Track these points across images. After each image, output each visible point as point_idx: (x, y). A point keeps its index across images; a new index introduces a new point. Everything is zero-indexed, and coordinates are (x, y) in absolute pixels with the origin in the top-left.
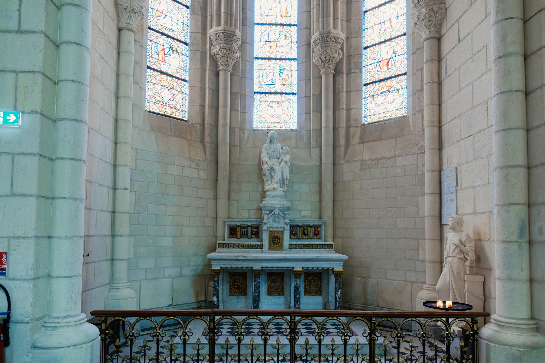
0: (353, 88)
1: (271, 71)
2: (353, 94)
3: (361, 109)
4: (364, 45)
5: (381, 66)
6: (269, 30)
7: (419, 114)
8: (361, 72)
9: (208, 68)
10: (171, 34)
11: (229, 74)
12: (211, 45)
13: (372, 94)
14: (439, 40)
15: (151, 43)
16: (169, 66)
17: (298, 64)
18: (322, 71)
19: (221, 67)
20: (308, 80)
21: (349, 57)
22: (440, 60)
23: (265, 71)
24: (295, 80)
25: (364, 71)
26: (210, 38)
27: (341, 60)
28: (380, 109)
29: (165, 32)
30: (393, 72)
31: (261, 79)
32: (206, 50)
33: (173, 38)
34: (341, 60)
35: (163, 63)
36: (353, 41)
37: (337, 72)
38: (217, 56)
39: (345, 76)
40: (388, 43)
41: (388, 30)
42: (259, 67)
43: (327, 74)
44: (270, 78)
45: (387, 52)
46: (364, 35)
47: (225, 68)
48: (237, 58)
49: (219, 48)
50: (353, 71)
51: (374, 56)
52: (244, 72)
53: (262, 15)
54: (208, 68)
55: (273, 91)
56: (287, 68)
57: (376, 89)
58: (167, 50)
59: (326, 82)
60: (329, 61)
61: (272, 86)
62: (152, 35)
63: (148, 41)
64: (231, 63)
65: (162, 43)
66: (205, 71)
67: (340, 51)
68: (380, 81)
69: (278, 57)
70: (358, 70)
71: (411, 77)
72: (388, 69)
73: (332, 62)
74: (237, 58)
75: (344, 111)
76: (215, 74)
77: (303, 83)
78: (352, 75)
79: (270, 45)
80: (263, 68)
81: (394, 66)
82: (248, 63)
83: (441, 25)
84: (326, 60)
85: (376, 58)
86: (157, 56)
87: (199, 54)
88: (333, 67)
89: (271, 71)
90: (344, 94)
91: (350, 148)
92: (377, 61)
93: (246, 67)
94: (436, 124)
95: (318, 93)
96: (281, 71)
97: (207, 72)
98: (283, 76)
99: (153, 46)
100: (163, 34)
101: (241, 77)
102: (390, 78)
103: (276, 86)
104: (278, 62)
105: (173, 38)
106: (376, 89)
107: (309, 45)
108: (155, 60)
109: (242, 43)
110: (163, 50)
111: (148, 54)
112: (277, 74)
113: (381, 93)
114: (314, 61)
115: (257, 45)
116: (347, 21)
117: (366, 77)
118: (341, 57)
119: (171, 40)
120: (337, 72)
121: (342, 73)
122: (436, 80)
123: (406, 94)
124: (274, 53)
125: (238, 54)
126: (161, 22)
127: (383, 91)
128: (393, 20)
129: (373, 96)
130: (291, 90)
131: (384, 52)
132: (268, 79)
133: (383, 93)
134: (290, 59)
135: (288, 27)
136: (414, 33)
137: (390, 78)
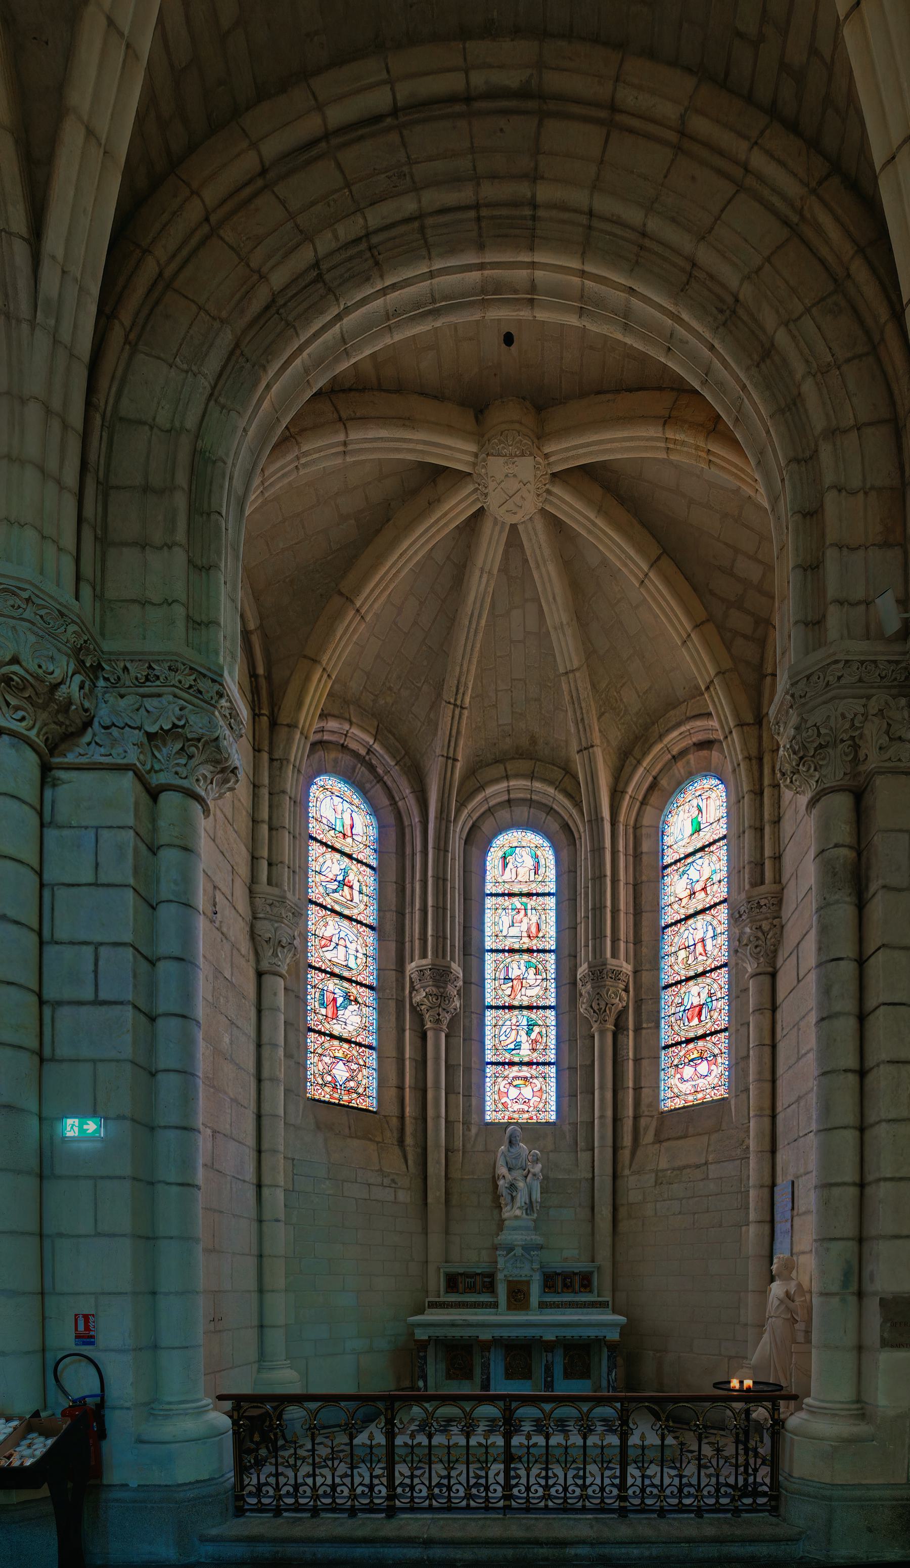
0: (645, 1053)
1: (514, 1027)
2: (645, 1063)
3: (658, 1087)
4: (663, 983)
5: (690, 1017)
6: (509, 960)
7: (744, 1096)
8: (658, 1026)
9: (408, 1027)
10: (346, 974)
11: (443, 1035)
12: (412, 988)
13: (675, 1063)
14: (773, 975)
15: (313, 990)
16: (343, 1026)
17: (557, 1016)
18: (595, 1026)
19: (428, 1025)
20: (573, 1040)
21: (639, 1002)
22: (774, 1009)
23: (504, 1028)
24: (552, 1043)
25: (663, 1025)
26: (411, 978)
27: (626, 1008)
28: (686, 1088)
29: (337, 971)
30: (708, 1026)
31: (497, 1042)
32: (404, 997)
33: (350, 981)
34: (626, 1008)
35: (335, 1021)
36: (645, 977)
37: (619, 1027)
38: (423, 1007)
39: (631, 1033)
40: (700, 980)
41: (700, 958)
42: (494, 1022)
43: (602, 1032)
44: (512, 1039)
45: (699, 994)
46: (662, 965)
47: (435, 1026)
48: (455, 1009)
49: (424, 994)
50: (644, 1025)
51: (678, 1000)
52: (467, 1030)
53: (497, 936)
54: (408, 1027)
55: (516, 1059)
56: (540, 1022)
57: (682, 1054)
58: (340, 1000)
59: (602, 1044)
60: (605, 1011)
61: (514, 1052)
62: (314, 977)
63: (309, 987)
64: (446, 1018)
65: (331, 987)
66: (404, 1030)
67: (623, 993)
68: (688, 1041)
69: (525, 1003)
70: (652, 1025)
71: (733, 1037)
72: (700, 1021)
73: (610, 1012)
74: (455, 1009)
75: (631, 1092)
76: (420, 1035)
77: (565, 1047)
78: (644, 1032)
79: (511, 984)
80: (500, 1023)
81: (708, 1017)
82: (474, 1016)
83: (775, 952)
84: (600, 1009)
85: (682, 1004)
86: (323, 1011)
87: (392, 1004)
88: (611, 1019)
89: (514, 1027)
90: (631, 1063)
91: (639, 1153)
92: (682, 1008)
93: (471, 1021)
94: (768, 1112)
95: (588, 1063)
96: (531, 1026)
97: (407, 1033)
98: (533, 1036)
99: (317, 995)
100: (333, 974)
101: (464, 1040)
102: (703, 1037)
103: (522, 1052)
104: (525, 1012)
105: (350, 981)
106: (682, 1054)
107: (574, 983)
108: (321, 1017)
109: (464, 982)
110: (335, 1000)
111: (309, 1008)
112: (523, 1034)
113: (690, 1061)
114: (582, 1010)
115: (489, 985)
116: (635, 944)
117: (666, 1037)
118: (625, 1004)
119: (346, 984)
120: (619, 1027)
121: (627, 1029)
122: (767, 1041)
123: (727, 1063)
124: (518, 997)
125: (457, 1003)
126: (329, 955)
127: (692, 1057)
128: (709, 943)
129: (677, 1066)
130: (547, 1057)
131: (695, 994)
132: (509, 1042)
133: (692, 1060)
134: (545, 1008)
135: (541, 955)
136: (737, 964)
137: (703, 1037)
